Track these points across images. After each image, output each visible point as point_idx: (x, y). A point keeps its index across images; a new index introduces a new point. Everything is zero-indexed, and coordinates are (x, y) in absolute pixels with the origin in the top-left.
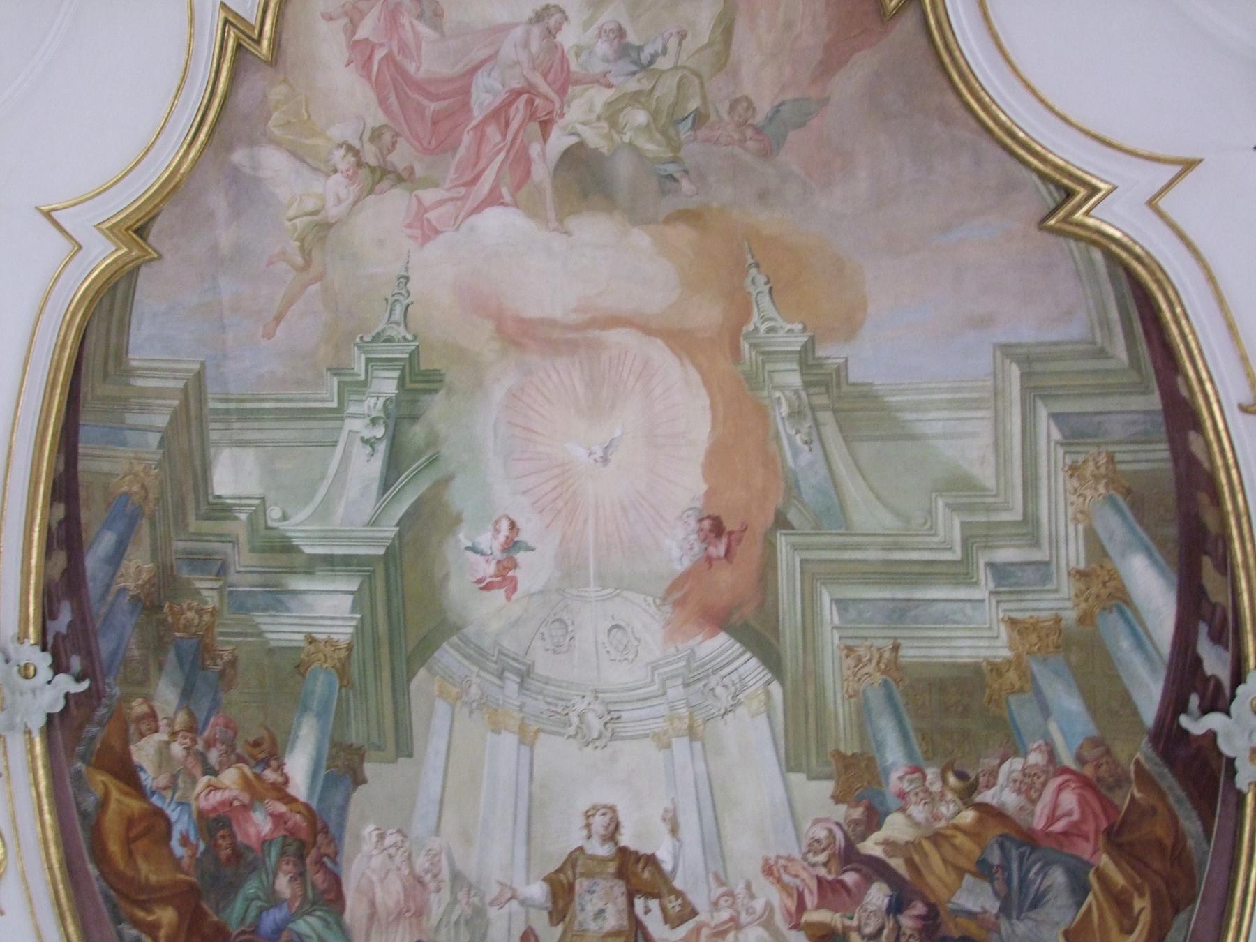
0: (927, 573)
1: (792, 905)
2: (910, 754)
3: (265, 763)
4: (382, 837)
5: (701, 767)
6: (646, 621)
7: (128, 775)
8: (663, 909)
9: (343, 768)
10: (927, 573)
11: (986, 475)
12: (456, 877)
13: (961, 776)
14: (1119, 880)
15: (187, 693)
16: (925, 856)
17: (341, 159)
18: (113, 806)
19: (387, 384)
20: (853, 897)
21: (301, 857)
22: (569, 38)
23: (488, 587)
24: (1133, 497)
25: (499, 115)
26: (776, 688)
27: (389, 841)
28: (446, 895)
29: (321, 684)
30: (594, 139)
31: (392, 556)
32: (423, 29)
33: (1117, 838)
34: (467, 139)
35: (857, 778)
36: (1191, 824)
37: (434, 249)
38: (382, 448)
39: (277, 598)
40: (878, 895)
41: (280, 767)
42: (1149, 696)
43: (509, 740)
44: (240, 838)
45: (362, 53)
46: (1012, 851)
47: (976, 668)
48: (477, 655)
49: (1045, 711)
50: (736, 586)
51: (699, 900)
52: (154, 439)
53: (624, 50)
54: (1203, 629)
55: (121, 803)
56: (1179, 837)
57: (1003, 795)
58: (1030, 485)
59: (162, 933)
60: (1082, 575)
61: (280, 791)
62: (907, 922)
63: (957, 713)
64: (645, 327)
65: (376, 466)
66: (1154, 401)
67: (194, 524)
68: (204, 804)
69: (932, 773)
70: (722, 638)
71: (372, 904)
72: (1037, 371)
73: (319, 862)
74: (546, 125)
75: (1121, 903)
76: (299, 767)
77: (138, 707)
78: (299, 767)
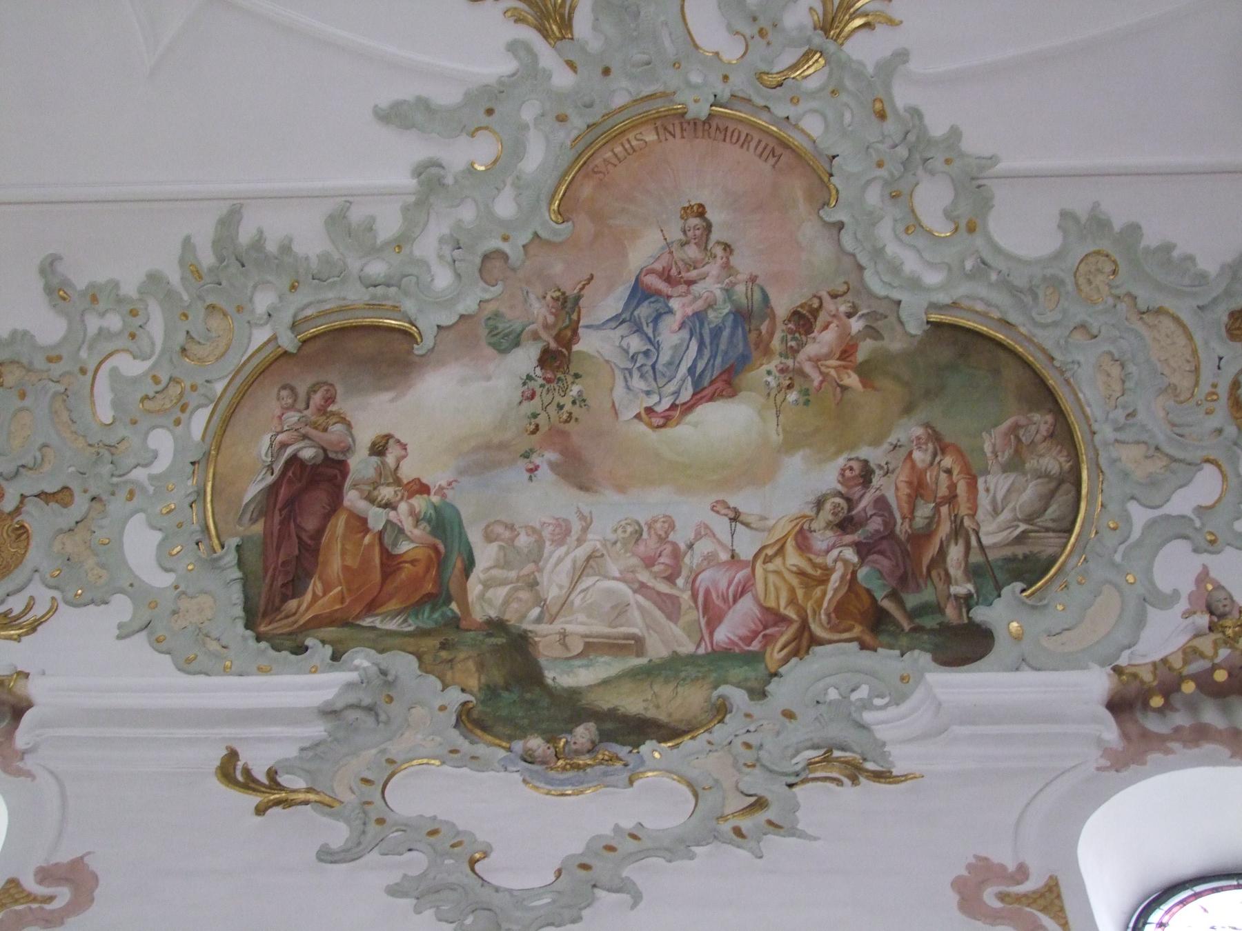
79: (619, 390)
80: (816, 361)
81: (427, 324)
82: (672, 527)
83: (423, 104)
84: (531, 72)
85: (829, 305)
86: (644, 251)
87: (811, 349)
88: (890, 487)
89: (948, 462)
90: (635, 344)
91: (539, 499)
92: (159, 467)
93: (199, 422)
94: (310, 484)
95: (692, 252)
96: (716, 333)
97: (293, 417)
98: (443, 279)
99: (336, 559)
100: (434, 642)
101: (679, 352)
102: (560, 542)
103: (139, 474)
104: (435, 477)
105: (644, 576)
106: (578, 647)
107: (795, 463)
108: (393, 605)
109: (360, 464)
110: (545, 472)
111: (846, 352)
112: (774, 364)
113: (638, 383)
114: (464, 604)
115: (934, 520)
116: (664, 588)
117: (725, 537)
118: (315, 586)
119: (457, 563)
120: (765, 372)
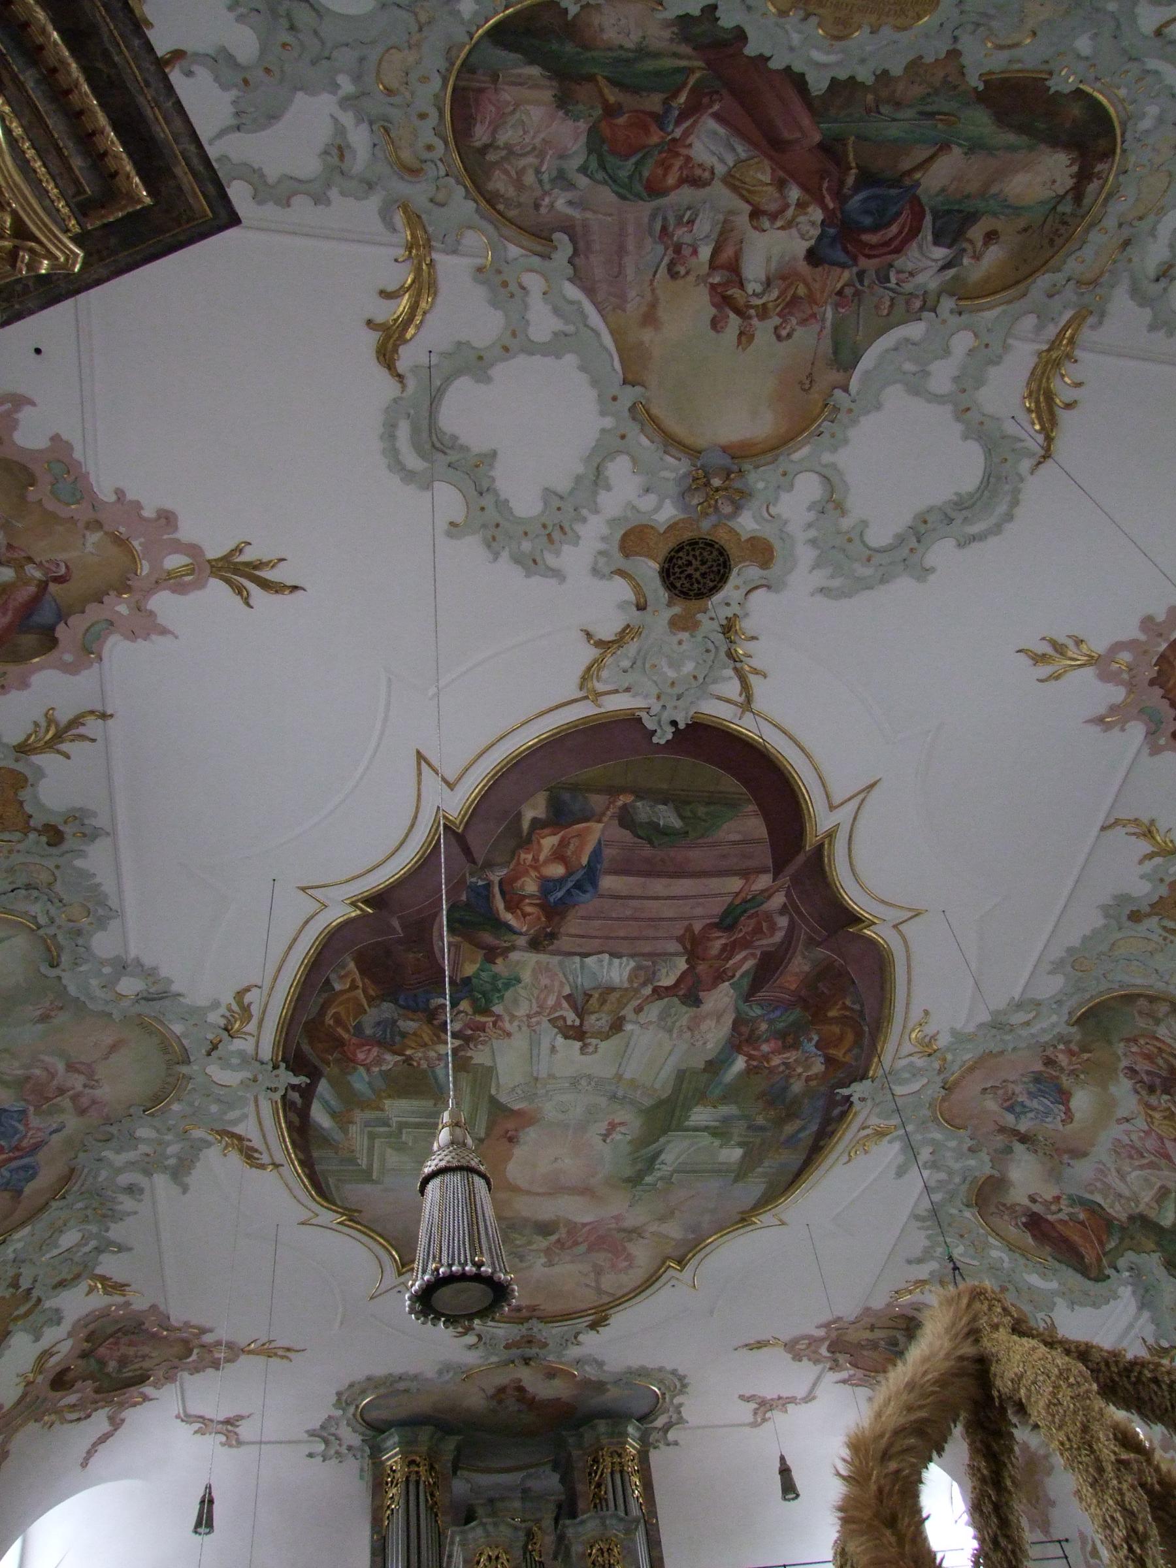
0: (418, 1126)
1: (500, 1023)
2: (433, 1072)
3: (755, 1067)
5: (535, 1068)
6: (549, 1110)
7: (829, 1061)
9: (714, 1066)
10: (418, 1126)
12: (670, 1031)
13: (410, 1065)
14: (339, 1030)
15: (785, 1089)
16: (432, 1040)
17: (647, 1235)
18: (843, 1051)
19: (648, 1179)
21: (750, 1036)
22: (543, 1260)
26: (493, 1092)
27: (701, 1043)
29: (718, 1092)
30: (541, 1238)
31: (665, 1132)
33: (340, 1043)
36: (306, 1047)
37: (616, 1213)
39: (726, 1120)
41: (748, 1065)
42: (323, 1087)
43: (627, 1076)
44: (780, 1043)
45: (629, 1258)
46: (389, 1039)
47: (399, 1097)
48: (632, 1102)
49: (369, 1083)
51: (546, 1024)
52: (766, 1164)
53: (522, 1258)
54: (299, 1106)
55: (838, 1053)
56: (311, 1043)
57: (391, 1059)
58: (371, 1149)
60: (351, 1122)
61: (751, 1057)
64: (528, 1193)
65: (663, 1157)
66: (317, 1168)
67: (758, 1141)
68: (794, 1053)
69: (424, 1065)
70: (516, 1107)
71: (718, 1021)
72: (366, 1176)
73: (740, 1034)
74: (558, 1241)
76: (740, 1064)
77: (813, 1083)
78: (740, 1064)
79: (1049, 1126)
80: (1070, 1063)
81: (988, 1171)
83: (899, 1167)
85: (1048, 1053)
86: (991, 1105)
87: (1064, 1064)
88: (1143, 1066)
89: (1142, 1042)
90: (1031, 1115)
91: (1082, 1171)
93: (991, 1240)
94: (1035, 1224)
95: (1000, 1092)
96: (1040, 1090)
97: (1006, 1217)
98: (972, 1162)
100: (1127, 1240)
101: (1044, 1105)
102: (1106, 1176)
103: (1006, 1265)
104: (1056, 1192)
105: (1137, 1163)
106: (1155, 1205)
107: (1113, 1089)
108: (1104, 1237)
109: (1036, 1208)
111: (1072, 1053)
112: (1064, 1078)
114: (1115, 1218)
115: (1166, 1061)
116: (1145, 1161)
117: (1134, 1128)
118: (1082, 1250)
119: (1096, 1208)
120: (1066, 1082)
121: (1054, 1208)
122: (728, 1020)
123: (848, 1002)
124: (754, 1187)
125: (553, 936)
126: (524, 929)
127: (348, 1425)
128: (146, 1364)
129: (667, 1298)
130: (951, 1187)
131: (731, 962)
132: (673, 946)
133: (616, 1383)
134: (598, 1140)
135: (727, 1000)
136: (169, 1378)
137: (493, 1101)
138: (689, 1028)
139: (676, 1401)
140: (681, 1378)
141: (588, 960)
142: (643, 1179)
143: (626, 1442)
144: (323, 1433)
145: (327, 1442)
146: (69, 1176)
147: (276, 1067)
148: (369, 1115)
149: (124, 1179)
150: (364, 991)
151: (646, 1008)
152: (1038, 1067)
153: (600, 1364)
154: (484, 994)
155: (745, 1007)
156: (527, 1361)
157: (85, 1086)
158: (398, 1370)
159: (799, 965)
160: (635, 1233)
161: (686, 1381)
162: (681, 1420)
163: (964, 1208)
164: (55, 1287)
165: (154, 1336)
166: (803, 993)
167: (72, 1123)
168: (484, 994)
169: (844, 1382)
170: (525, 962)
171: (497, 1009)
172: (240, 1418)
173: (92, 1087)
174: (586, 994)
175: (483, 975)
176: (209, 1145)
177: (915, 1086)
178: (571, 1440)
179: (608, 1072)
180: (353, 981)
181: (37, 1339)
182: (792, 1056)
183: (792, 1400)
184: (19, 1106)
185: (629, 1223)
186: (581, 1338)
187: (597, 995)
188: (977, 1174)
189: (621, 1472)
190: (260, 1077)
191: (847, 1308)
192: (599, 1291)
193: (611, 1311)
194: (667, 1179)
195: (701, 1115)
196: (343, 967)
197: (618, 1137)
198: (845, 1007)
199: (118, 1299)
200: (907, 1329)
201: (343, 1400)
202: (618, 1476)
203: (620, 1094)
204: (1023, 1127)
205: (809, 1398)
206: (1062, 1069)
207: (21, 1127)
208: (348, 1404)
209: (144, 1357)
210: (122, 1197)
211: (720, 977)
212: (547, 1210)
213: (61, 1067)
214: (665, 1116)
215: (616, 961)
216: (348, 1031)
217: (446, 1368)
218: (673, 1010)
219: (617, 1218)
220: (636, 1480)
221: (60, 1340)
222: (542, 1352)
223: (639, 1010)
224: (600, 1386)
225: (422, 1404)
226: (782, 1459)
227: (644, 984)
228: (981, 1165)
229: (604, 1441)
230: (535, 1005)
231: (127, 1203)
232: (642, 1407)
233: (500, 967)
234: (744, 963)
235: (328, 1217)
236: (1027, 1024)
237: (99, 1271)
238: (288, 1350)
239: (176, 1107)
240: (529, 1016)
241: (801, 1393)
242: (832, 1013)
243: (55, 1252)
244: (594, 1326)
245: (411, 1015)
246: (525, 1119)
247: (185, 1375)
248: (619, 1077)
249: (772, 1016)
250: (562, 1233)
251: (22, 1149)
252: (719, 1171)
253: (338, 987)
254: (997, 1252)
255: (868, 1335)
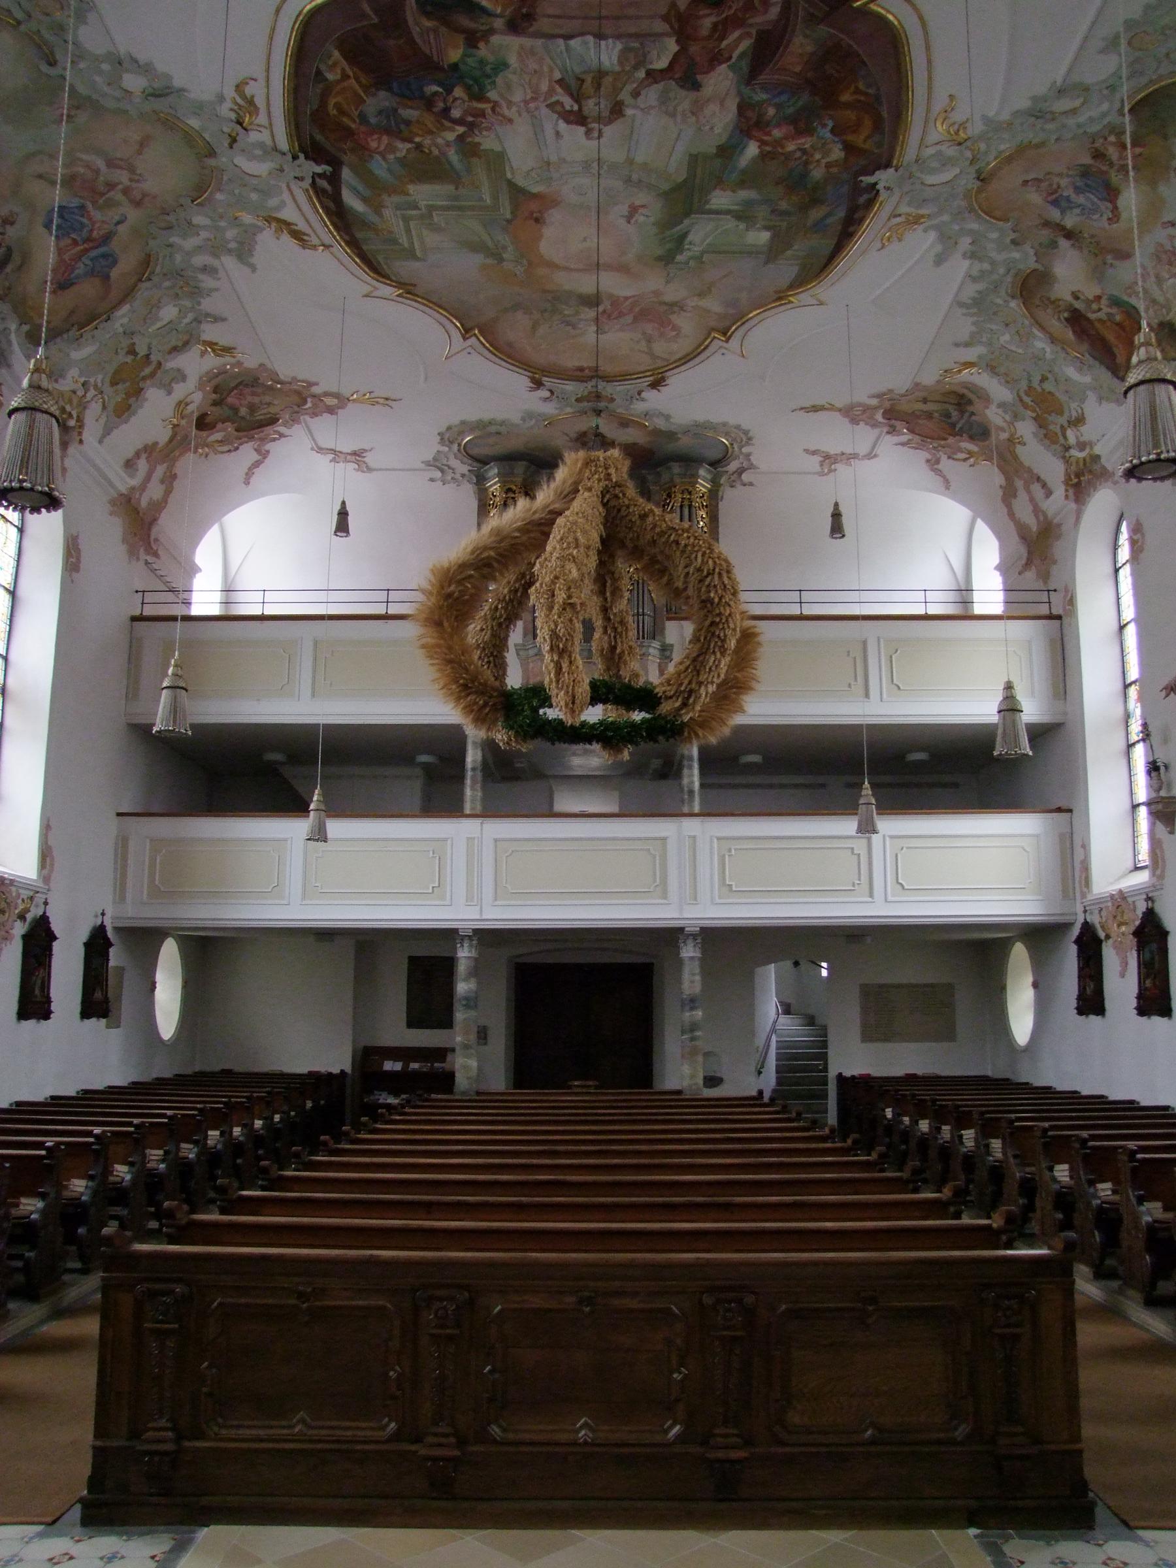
0: (448, 208)
1: (497, 109)
4: (712, 128)
7: (849, 148)
8: (563, 107)
9: (727, 152)
10: (448, 208)
11: (425, 232)
14: (345, 119)
15: (804, 175)
18: (862, 137)
19: (679, 258)
20: (467, 112)
23: (643, 206)
24: (365, 225)
25: (621, 315)
26: (509, 176)
28: (680, 109)
31: (687, 214)
32: (650, 332)
33: (349, 133)
34: (637, 309)
35: (469, 149)
36: (319, 137)
38: (686, 242)
39: (749, 204)
40: (456, 113)
42: (346, 173)
43: (640, 158)
44: (791, 128)
46: (395, 128)
49: (389, 170)
50: (528, 207)
51: (545, 111)
52: (796, 247)
53: (574, 327)
55: (859, 140)
57: (403, 148)
58: (408, 231)
59: (852, 89)
60: (383, 207)
61: (763, 143)
62: (441, 105)
63: (427, 168)
65: (690, 238)
66: (365, 248)
68: (809, 139)
69: (436, 152)
70: (535, 189)
74: (604, 311)
75: (342, 112)
77: (834, 170)
81: (1031, 264)
82: (1162, 245)
84: (936, 228)
85: (1097, 145)
86: (1035, 197)
90: (1077, 211)
92: (1048, 350)
93: (1036, 332)
94: (1077, 320)
95: (1044, 185)
96: (1087, 185)
99: (1111, 337)
103: (1048, 356)
104: (1098, 292)
109: (1078, 305)
110: (1116, 263)
113: (1096, 217)
118: (1116, 350)
120: (1115, 178)
121: (1095, 306)
122: (732, 105)
123: (861, 86)
124: (786, 270)
125: (530, 17)
126: (499, 11)
127: (456, 458)
128: (273, 410)
129: (719, 364)
130: (995, 277)
131: (725, 43)
132: (660, 26)
133: (686, 432)
134: (623, 221)
135: (728, 83)
136: (295, 421)
137: (511, 184)
138: (693, 113)
139: (744, 450)
140: (746, 432)
141: (572, 43)
142: (674, 258)
143: (697, 482)
144: (436, 463)
145: (442, 471)
146: (147, 262)
147: (295, 158)
148: (396, 199)
149: (199, 260)
150: (357, 79)
151: (643, 92)
152: (1087, 160)
153: (668, 417)
154: (476, 80)
155: (746, 91)
156: (598, 413)
157: (131, 180)
158: (500, 416)
159: (801, 45)
160: (677, 306)
161: (751, 434)
162: (752, 467)
163: (1009, 299)
164: (170, 353)
165: (271, 388)
166: (809, 75)
167: (133, 215)
168: (476, 80)
169: (903, 444)
170: (507, 46)
171: (492, 95)
172: (365, 451)
173: (138, 181)
174: (578, 79)
175: (470, 60)
176: (261, 230)
177: (947, 176)
178: (650, 478)
179: (618, 156)
180: (343, 70)
181: (169, 393)
182: (807, 142)
183: (855, 456)
184: (75, 202)
185: (668, 298)
186: (644, 395)
187: (589, 80)
188: (1022, 266)
189: (690, 506)
190: (285, 167)
191: (899, 381)
192: (654, 357)
193: (668, 374)
194: (699, 259)
195: (720, 199)
196: (330, 57)
197: (642, 219)
198: (857, 91)
199: (228, 359)
200: (959, 404)
201: (448, 437)
202: (686, 511)
203: (635, 177)
204: (1069, 222)
205: (871, 456)
206: (1111, 165)
207: (85, 220)
208: (451, 442)
209: (269, 404)
210: (201, 276)
211: (716, 59)
212: (586, 284)
213: (101, 164)
214: (684, 199)
215: (603, 43)
216: (355, 122)
217: (529, 415)
218: (672, 95)
219: (657, 293)
220: (703, 513)
221: (192, 393)
222: (612, 406)
223: (636, 94)
224: (671, 435)
225: (515, 444)
226: (836, 504)
227: (636, 67)
228: (1025, 259)
229: (677, 480)
230: (529, 91)
231: (207, 282)
232: (714, 454)
233: (483, 51)
234: (740, 43)
235: (387, 290)
236: (1074, 111)
237: (206, 337)
238: (387, 399)
239: (219, 196)
240: (526, 102)
241: (863, 450)
242: (846, 97)
243: (159, 325)
244: (656, 384)
245: (410, 103)
246: (546, 202)
247: (307, 418)
248: (630, 162)
249: (777, 100)
250: (605, 305)
251: (95, 240)
252: (751, 252)
253: (330, 77)
254: (1040, 343)
255: (920, 406)
